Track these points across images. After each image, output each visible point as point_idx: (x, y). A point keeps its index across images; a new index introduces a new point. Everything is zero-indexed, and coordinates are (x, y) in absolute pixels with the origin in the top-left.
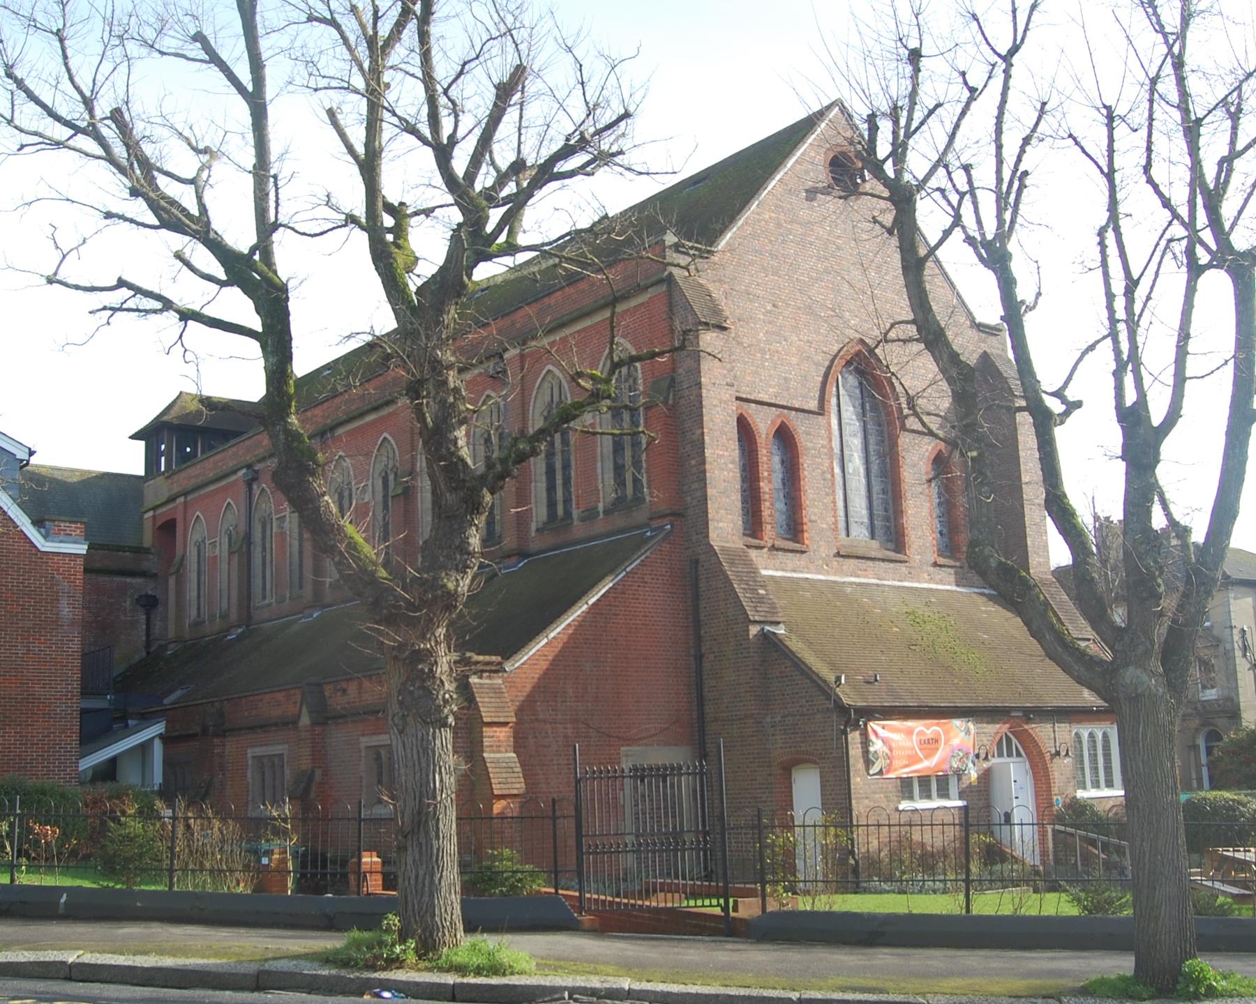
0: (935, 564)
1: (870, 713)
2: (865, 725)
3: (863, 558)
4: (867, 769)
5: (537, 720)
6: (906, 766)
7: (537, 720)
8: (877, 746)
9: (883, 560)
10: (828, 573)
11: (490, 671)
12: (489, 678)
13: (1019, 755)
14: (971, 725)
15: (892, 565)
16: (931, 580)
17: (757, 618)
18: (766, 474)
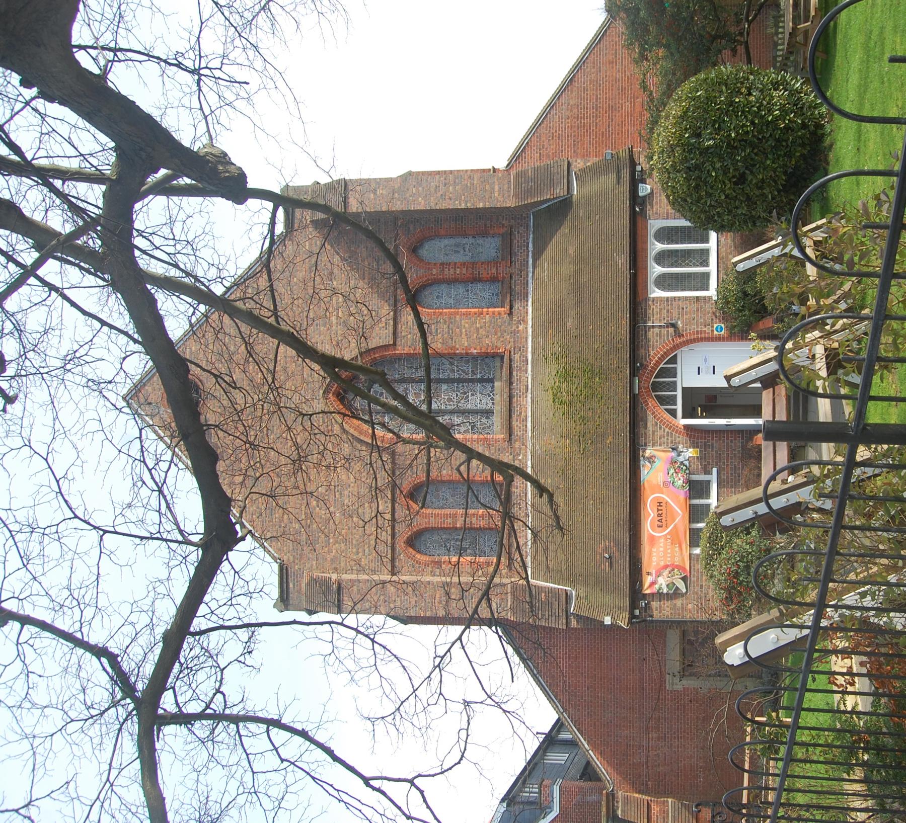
0: (511, 314)
1: (636, 594)
2: (645, 596)
3: (510, 410)
4: (683, 595)
5: (647, 763)
6: (680, 547)
7: (647, 763)
8: (662, 583)
9: (511, 383)
10: (525, 455)
11: (613, 800)
12: (618, 802)
13: (674, 360)
14: (648, 453)
15: (515, 373)
16: (526, 323)
17: (564, 621)
18: (450, 520)
